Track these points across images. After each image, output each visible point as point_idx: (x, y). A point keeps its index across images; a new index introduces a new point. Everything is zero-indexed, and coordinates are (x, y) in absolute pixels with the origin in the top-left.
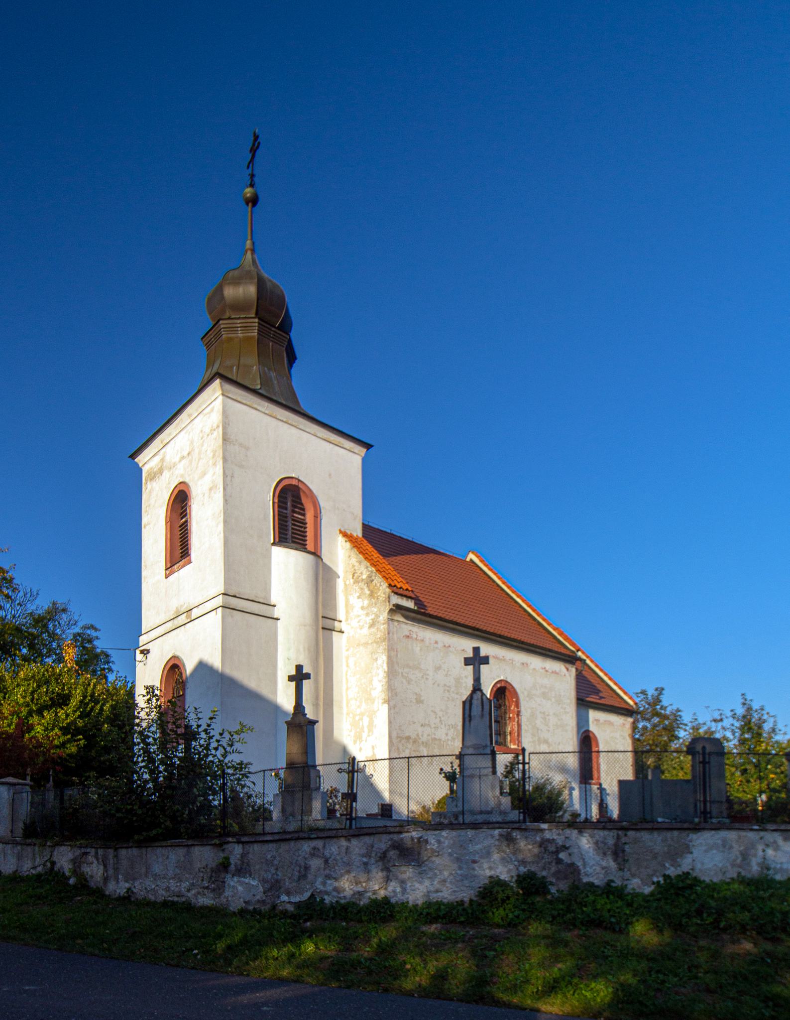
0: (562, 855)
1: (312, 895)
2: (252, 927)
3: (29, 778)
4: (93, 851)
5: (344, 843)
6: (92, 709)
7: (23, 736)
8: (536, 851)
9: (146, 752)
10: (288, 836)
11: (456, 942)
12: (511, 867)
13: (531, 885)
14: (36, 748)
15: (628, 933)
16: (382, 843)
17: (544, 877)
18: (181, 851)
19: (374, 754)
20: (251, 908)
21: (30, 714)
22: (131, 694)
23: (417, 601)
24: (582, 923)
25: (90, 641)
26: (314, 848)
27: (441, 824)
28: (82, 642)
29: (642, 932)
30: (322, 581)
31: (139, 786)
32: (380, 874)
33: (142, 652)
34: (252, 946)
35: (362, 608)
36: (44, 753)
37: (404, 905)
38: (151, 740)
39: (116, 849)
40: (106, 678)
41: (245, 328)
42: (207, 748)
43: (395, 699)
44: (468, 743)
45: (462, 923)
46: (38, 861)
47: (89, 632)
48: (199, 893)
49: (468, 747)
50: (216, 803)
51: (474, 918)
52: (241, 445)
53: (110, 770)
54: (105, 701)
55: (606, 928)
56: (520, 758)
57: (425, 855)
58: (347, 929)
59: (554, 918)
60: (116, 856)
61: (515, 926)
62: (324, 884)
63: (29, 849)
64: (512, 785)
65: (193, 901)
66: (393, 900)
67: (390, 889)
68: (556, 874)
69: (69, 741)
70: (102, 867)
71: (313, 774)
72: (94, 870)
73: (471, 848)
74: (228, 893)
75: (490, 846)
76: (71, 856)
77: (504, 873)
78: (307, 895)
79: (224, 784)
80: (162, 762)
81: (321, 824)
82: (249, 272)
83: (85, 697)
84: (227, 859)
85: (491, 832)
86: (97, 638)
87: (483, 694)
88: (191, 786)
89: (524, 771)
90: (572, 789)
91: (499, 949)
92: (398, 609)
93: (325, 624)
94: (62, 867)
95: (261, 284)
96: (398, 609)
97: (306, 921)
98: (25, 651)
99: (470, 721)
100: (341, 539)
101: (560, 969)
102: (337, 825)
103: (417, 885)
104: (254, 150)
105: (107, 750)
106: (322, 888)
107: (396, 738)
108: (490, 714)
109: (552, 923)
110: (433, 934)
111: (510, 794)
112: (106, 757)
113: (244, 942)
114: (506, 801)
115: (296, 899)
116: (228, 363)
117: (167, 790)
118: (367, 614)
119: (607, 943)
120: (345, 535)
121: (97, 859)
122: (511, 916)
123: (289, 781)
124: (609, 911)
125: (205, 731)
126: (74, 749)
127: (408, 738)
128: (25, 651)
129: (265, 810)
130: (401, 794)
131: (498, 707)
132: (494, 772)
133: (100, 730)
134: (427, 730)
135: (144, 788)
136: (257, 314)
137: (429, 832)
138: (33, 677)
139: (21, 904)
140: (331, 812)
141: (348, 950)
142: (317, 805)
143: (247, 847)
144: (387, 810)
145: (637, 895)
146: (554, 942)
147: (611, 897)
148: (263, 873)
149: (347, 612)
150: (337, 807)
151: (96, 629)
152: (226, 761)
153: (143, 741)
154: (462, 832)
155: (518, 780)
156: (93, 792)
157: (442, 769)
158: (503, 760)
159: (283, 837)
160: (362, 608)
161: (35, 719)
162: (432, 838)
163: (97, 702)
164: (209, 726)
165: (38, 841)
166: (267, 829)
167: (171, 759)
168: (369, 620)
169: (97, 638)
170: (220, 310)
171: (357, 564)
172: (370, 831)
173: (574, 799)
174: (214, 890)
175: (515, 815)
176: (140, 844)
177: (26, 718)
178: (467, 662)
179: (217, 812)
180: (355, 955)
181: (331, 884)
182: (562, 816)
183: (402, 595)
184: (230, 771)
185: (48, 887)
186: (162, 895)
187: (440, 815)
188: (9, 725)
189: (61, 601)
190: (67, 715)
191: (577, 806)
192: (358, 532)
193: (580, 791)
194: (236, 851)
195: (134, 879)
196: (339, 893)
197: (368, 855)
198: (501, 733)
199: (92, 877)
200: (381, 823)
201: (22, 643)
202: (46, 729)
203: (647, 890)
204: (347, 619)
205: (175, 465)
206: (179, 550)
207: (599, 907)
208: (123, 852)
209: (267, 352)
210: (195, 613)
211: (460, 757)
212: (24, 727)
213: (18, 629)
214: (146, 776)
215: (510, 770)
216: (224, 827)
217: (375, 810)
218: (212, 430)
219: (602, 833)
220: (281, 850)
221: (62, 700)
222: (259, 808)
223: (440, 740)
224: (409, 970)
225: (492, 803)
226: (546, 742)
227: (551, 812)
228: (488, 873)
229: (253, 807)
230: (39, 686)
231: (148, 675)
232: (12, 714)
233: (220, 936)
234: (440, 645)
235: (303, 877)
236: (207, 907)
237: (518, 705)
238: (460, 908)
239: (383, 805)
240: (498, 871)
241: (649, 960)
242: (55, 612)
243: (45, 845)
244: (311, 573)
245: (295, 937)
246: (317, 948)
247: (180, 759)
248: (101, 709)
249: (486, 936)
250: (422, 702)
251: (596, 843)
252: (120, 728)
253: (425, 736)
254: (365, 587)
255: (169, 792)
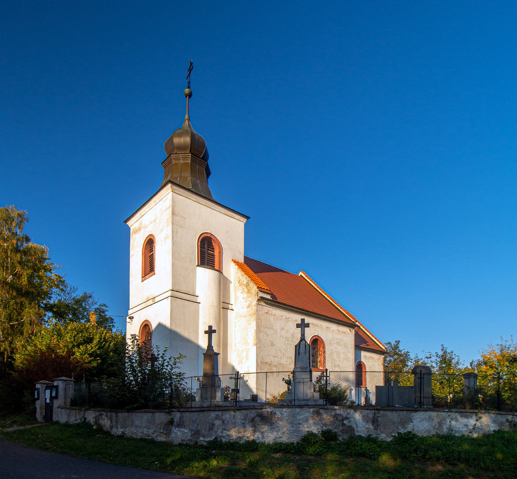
0: (345, 422)
1: (216, 438)
2: (185, 452)
3: (73, 377)
4: (105, 413)
5: (232, 413)
6: (104, 345)
7: (70, 358)
8: (332, 419)
9: (132, 366)
10: (203, 409)
11: (290, 462)
12: (319, 427)
13: (328, 436)
14: (76, 363)
15: (378, 460)
16: (252, 414)
17: (335, 432)
18: (149, 415)
19: (248, 371)
20: (185, 443)
21: (73, 347)
22: (124, 338)
23: (272, 296)
24: (355, 454)
25: (103, 312)
26: (217, 415)
27: (283, 405)
28: (99, 313)
29: (386, 460)
30: (223, 284)
31: (128, 383)
32: (251, 428)
33: (130, 318)
34: (185, 461)
35: (243, 298)
36: (81, 366)
37: (263, 444)
38: (134, 361)
39: (116, 413)
40: (111, 330)
41: (184, 158)
42: (163, 365)
43: (259, 344)
44: (297, 366)
45: (292, 453)
46: (78, 417)
47: (103, 307)
48: (158, 435)
49: (298, 368)
50: (167, 392)
51: (298, 451)
52: (181, 216)
53: (114, 375)
54: (111, 341)
55: (367, 457)
56: (325, 374)
57: (274, 420)
58: (233, 455)
59: (340, 452)
60: (117, 416)
61: (320, 455)
62: (222, 432)
63: (74, 411)
64: (320, 387)
65: (155, 439)
66: (257, 441)
67: (256, 436)
68: (343, 431)
69: (93, 360)
70: (109, 421)
71: (217, 379)
72: (106, 422)
73: (298, 417)
74: (173, 435)
75: (308, 417)
76: (94, 415)
77: (315, 430)
78: (213, 438)
79: (171, 383)
80: (140, 372)
81: (221, 404)
82: (187, 130)
83: (101, 339)
84: (173, 419)
85: (309, 410)
86: (107, 311)
87: (306, 342)
88: (154, 383)
89: (326, 380)
90: (351, 390)
91: (311, 466)
92: (262, 299)
93: (224, 306)
94: (89, 420)
95: (193, 137)
96: (262, 299)
97: (213, 450)
98: (70, 316)
99: (299, 355)
100: (233, 264)
101: (342, 476)
102: (229, 404)
103: (270, 434)
104: (190, 70)
105: (112, 365)
106: (221, 434)
107: (260, 363)
108: (309, 352)
109: (339, 454)
110: (278, 458)
111: (319, 391)
112: (112, 368)
113: (181, 459)
114: (317, 395)
115: (208, 439)
116: (175, 175)
117: (143, 385)
118: (246, 301)
119: (368, 464)
120: (235, 262)
121: (107, 417)
122: (318, 450)
123: (205, 382)
124: (369, 449)
125: (162, 357)
126: (95, 364)
127: (266, 363)
128: (70, 316)
129: (192, 396)
130: (262, 390)
131: (314, 349)
132: (311, 381)
133: (108, 355)
134: (276, 359)
135: (130, 384)
136: (190, 151)
137: (277, 409)
138: (75, 329)
139: (70, 437)
140: (226, 398)
141: (234, 464)
142: (219, 395)
143: (183, 414)
144: (255, 398)
145: (384, 442)
146: (340, 464)
147: (370, 443)
148: (191, 426)
149: (235, 300)
150: (229, 395)
151: (106, 307)
152: (172, 372)
153: (130, 361)
154: (294, 410)
155: (323, 385)
156: (105, 385)
157: (284, 379)
158: (316, 375)
159: (201, 410)
160: (243, 298)
161: (76, 349)
162: (278, 412)
163: (107, 342)
164: (164, 354)
165: (78, 408)
166: (193, 405)
167: (144, 370)
168: (247, 304)
169: (107, 311)
170: (171, 149)
171: (241, 277)
172: (246, 407)
173: (352, 395)
174: (166, 434)
175: (321, 402)
176: (129, 411)
177: (71, 349)
178: (298, 326)
179: (167, 396)
180: (237, 467)
181: (226, 433)
182: (346, 403)
183: (264, 292)
184: (174, 377)
185: (83, 430)
186: (139, 435)
187: (282, 401)
188: (63, 352)
189: (89, 292)
190: (92, 348)
191: (354, 398)
192: (242, 260)
193: (355, 391)
194: (177, 416)
195: (126, 427)
196: (229, 437)
197: (245, 419)
198: (315, 361)
199: (104, 426)
200: (252, 404)
201: (69, 313)
202: (81, 354)
203: (389, 440)
204: (235, 304)
205: (147, 226)
206: (149, 268)
207: (364, 447)
208: (120, 414)
209: (197, 171)
210: (157, 299)
211: (293, 373)
212: (70, 353)
213: (67, 306)
214: (132, 378)
215: (319, 380)
216: (171, 404)
217: (249, 398)
218: (167, 209)
219: (366, 411)
220: (200, 416)
221: (89, 340)
222: (189, 395)
223: (283, 364)
224: (265, 475)
225: (310, 395)
226: (338, 366)
227: (340, 401)
228: (307, 429)
229: (186, 395)
230: (78, 334)
231: (133, 329)
232: (65, 346)
233: (169, 456)
234: (284, 317)
235: (211, 429)
236: (162, 442)
237: (324, 348)
238: (292, 446)
239: (253, 395)
240: (312, 429)
241: (388, 473)
242: (86, 297)
243: (81, 410)
244: (217, 280)
245: (207, 457)
246: (218, 463)
247: (149, 370)
248: (109, 345)
249: (305, 460)
250: (274, 345)
251: (363, 416)
252: (119, 354)
253: (275, 362)
254: (245, 288)
255: (143, 386)
